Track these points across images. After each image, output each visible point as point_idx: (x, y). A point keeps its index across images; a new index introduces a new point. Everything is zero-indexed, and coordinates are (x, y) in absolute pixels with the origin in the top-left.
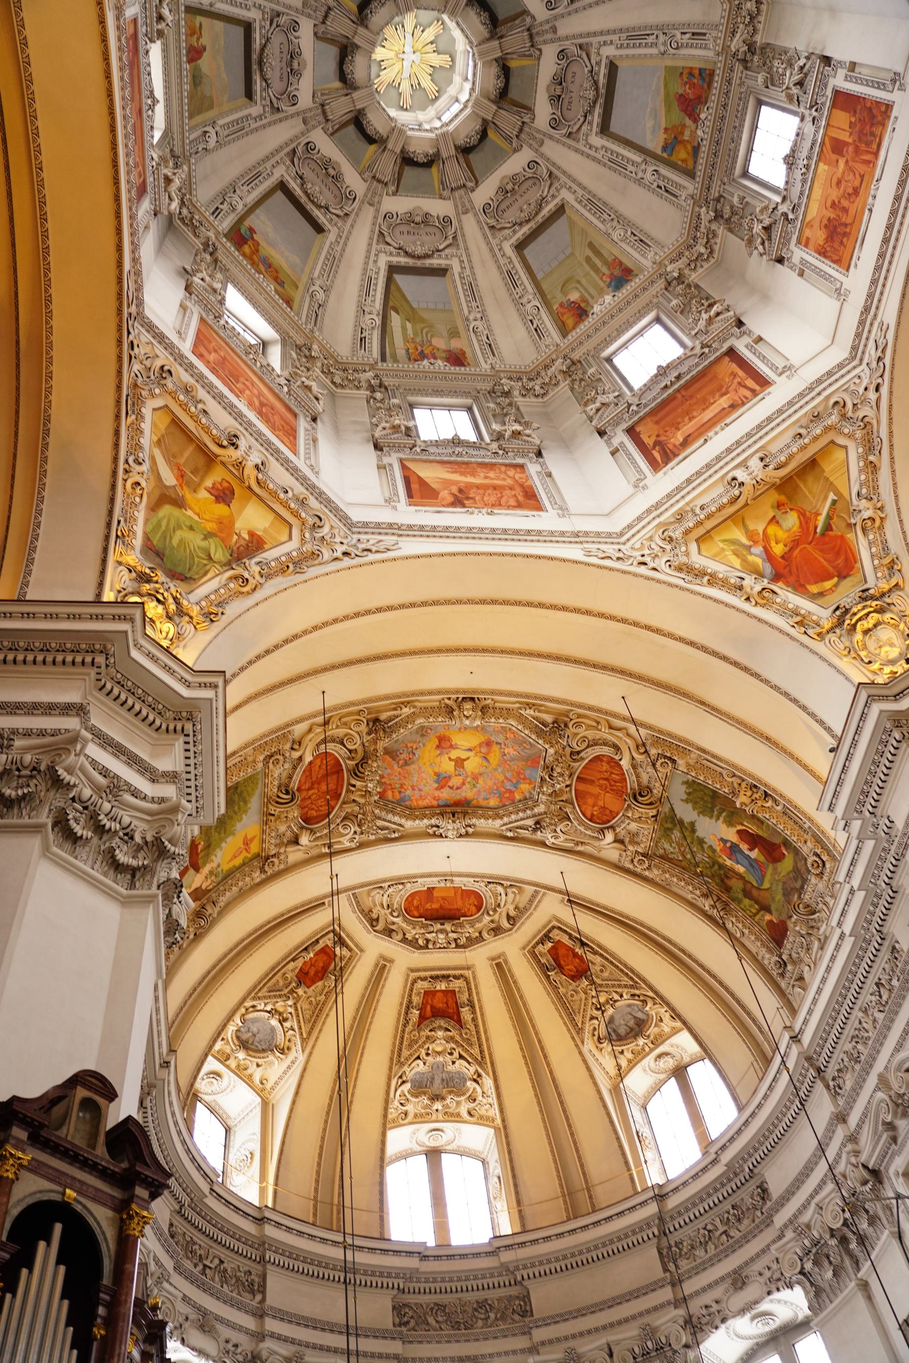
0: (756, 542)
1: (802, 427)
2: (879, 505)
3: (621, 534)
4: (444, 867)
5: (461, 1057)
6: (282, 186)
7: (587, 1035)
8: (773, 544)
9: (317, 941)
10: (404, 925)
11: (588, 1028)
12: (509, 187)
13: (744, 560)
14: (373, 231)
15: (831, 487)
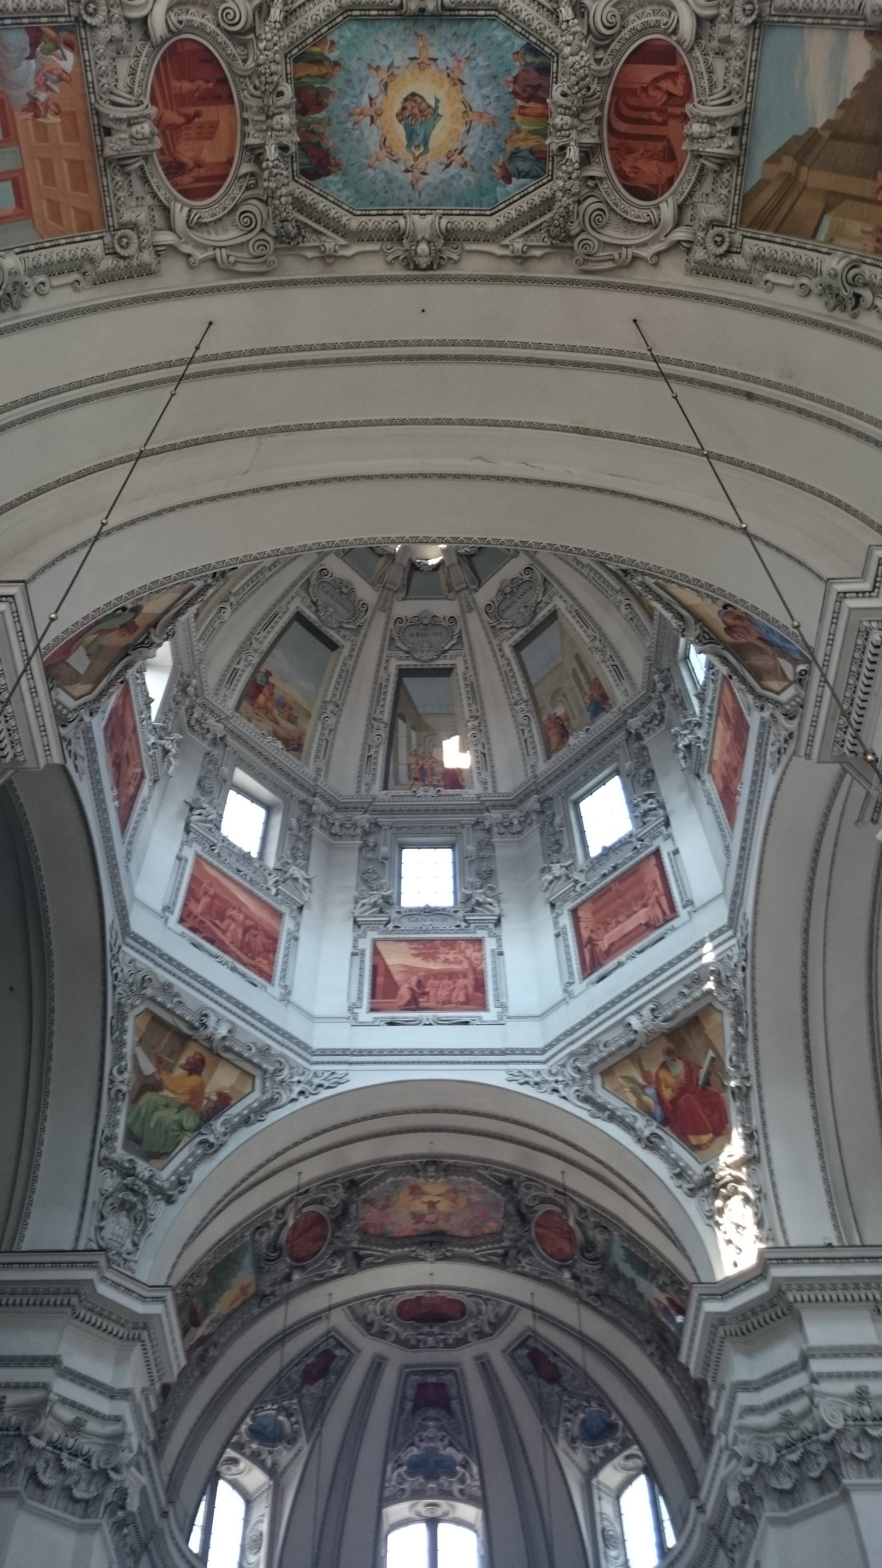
0: (649, 1083)
1: (686, 986)
2: (746, 1074)
3: (543, 1051)
4: (427, 1281)
5: (451, 1444)
6: (299, 617)
7: (561, 1434)
8: (663, 1088)
9: (318, 1347)
10: (396, 1328)
11: (562, 1429)
12: (508, 590)
13: (640, 1101)
14: (384, 637)
15: (710, 1045)
